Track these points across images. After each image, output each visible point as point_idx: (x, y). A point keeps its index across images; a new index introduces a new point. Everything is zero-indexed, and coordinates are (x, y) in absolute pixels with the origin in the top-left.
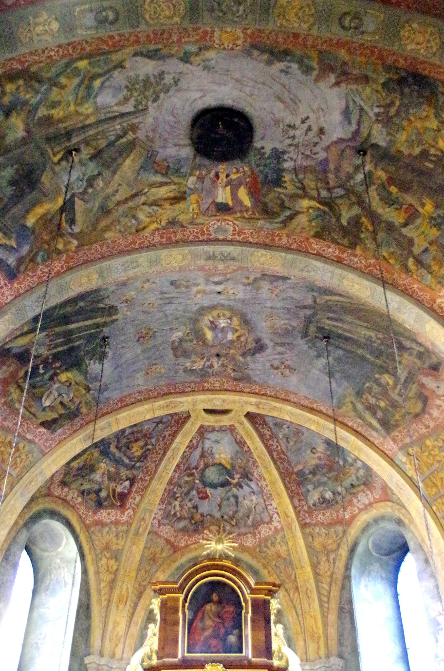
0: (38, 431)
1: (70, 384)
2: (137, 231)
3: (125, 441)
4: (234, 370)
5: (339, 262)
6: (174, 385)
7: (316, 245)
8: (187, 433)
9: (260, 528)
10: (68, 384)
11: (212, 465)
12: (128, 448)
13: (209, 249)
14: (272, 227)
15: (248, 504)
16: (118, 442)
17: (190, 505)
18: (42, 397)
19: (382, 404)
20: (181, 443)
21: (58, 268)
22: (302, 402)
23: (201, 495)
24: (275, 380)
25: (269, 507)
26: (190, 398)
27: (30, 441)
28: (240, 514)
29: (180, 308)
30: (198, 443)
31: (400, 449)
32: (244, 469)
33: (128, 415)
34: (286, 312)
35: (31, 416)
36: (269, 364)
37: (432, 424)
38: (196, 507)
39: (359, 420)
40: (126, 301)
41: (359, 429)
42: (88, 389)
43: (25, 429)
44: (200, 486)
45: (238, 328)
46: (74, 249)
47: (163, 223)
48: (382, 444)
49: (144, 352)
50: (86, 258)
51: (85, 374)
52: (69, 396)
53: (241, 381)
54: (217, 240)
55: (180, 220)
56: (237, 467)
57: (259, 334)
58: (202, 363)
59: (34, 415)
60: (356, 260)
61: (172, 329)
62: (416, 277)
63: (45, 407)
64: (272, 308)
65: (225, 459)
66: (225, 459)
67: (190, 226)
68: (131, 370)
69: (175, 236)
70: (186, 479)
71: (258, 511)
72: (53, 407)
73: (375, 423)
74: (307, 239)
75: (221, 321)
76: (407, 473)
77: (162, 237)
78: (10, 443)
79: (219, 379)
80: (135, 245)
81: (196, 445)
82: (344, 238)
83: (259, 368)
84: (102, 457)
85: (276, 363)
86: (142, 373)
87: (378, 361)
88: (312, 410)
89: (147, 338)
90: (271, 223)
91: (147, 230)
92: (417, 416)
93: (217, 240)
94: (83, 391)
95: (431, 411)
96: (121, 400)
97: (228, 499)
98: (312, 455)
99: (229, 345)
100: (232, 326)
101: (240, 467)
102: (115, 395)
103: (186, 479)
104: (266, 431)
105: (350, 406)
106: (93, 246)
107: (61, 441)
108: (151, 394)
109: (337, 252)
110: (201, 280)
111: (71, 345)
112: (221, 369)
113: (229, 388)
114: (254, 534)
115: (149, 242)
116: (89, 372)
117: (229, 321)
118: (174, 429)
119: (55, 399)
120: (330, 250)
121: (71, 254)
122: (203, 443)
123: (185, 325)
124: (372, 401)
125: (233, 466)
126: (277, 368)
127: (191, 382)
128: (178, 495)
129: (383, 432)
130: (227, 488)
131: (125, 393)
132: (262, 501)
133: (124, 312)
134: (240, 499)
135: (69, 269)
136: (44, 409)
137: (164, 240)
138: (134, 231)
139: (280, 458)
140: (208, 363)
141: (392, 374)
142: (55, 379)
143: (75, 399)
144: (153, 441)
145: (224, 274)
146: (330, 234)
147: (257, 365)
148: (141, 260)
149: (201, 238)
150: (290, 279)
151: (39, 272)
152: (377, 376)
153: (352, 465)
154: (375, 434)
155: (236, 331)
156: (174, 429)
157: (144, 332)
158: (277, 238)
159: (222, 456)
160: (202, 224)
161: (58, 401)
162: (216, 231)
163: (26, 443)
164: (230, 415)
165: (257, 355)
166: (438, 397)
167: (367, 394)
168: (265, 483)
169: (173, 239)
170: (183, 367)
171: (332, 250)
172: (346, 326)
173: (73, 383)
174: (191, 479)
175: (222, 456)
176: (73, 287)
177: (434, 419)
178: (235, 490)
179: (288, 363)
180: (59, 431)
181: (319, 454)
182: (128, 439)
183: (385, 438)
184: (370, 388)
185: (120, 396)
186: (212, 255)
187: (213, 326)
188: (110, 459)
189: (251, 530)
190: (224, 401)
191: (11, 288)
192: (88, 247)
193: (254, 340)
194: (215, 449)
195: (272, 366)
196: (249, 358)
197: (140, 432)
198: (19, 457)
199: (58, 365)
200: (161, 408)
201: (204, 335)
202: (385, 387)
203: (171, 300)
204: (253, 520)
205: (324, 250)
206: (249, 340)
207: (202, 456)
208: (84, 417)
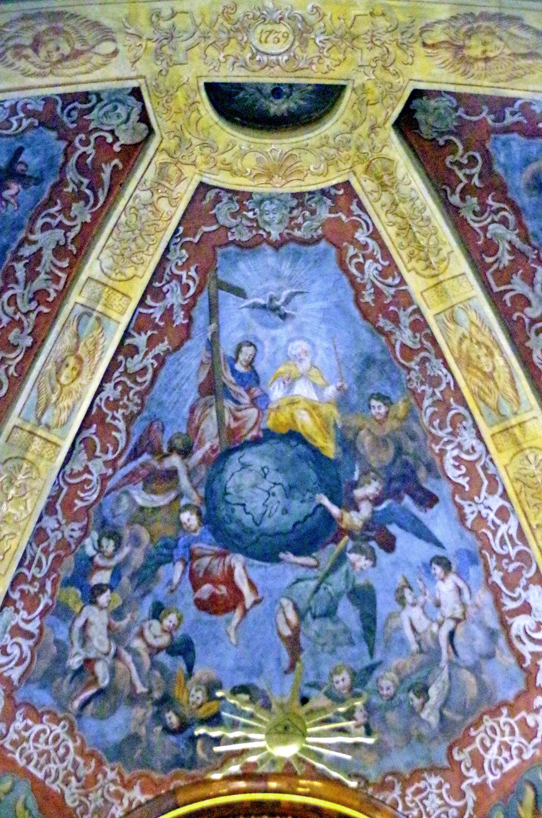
8: (140, 232)
9: (478, 734)
11: (257, 441)
15: (422, 624)
17: (156, 633)
20: (113, 282)
23: (206, 589)
25: (519, 624)
28: (387, 681)
30: (188, 309)
32: (399, 451)
38: (183, 649)
44: (206, 546)
56: (365, 441)
65: (313, 409)
66: (313, 409)
70: (142, 498)
71: (466, 656)
81: (180, 319)
97: (329, 613)
101: (380, 442)
103: (142, 498)
114: (452, 771)
118: (81, 213)
122: (213, 311)
125: (348, 444)
128: (102, 577)
130: (326, 555)
132: (484, 597)
134: (385, 605)
156: (81, 213)
159: (303, 390)
164: (331, 127)
168: (496, 502)
174: (161, 500)
175: (303, 390)
178: (359, 561)
189: (439, 752)
194: (267, 349)
204: (446, 703)
207: (210, 388)
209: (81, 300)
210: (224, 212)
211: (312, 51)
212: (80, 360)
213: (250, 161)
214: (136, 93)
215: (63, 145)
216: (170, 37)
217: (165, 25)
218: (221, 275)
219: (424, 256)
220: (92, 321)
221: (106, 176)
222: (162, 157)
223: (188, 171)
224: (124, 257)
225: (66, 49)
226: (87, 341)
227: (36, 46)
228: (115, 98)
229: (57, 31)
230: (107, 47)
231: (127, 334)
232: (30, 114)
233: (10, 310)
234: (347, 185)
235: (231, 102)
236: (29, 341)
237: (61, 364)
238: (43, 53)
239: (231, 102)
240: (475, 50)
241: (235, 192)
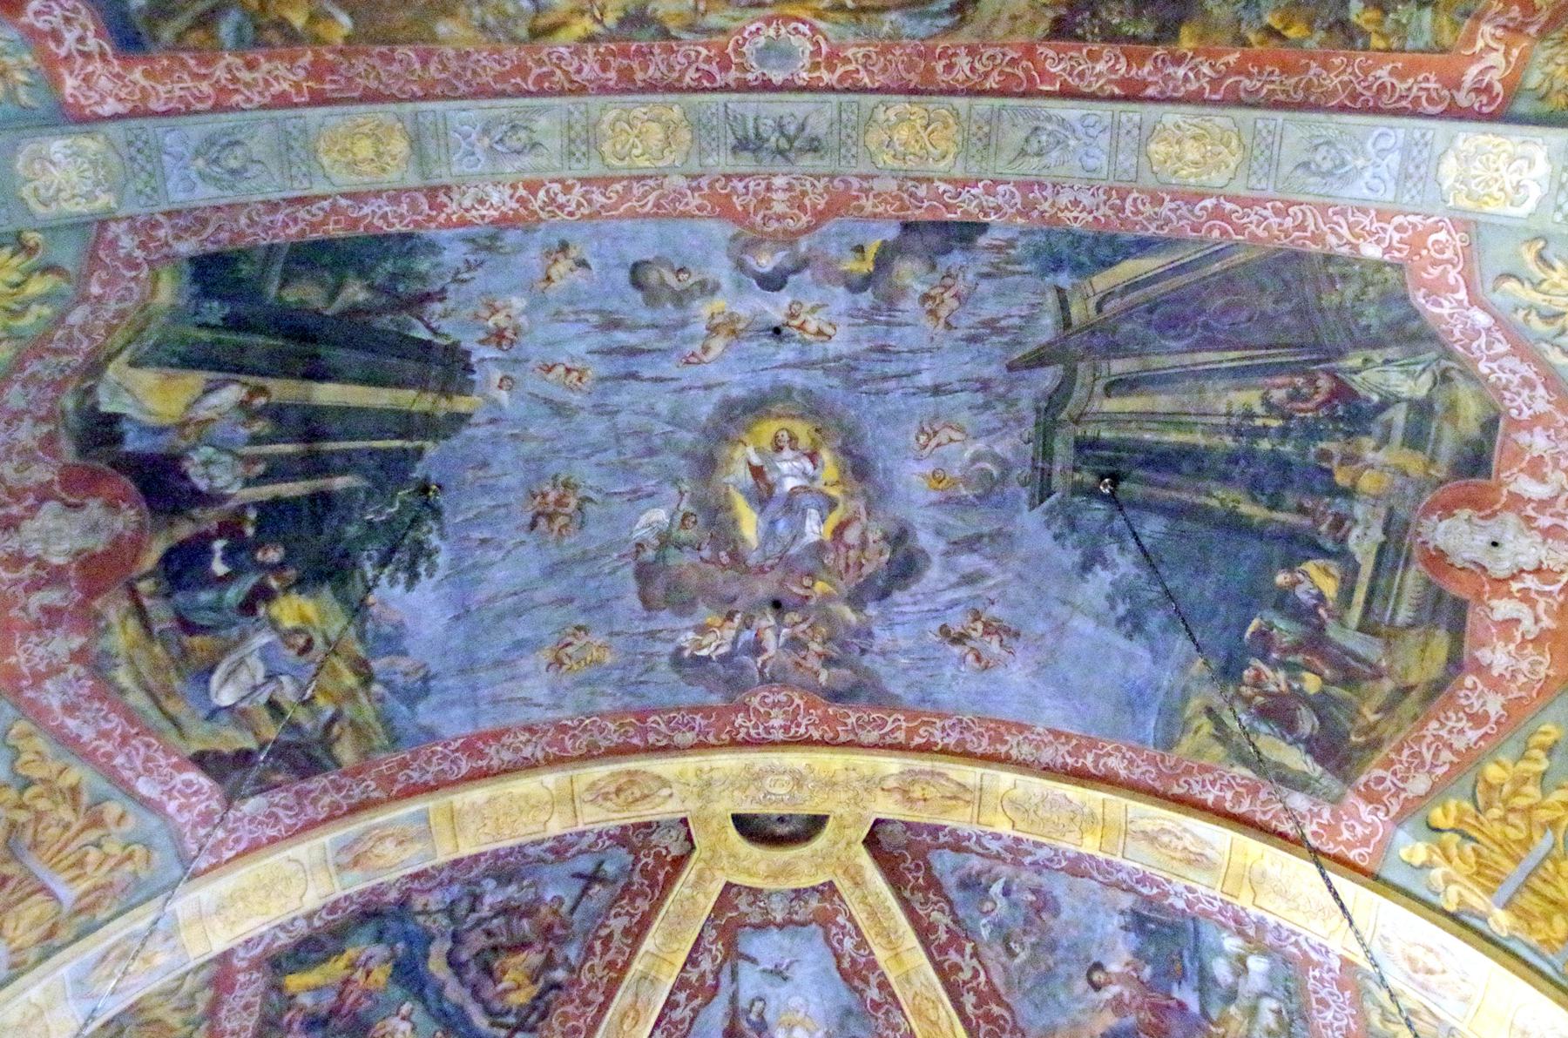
1: (310, 642)
2: (536, 34)
3: (477, 941)
4: (828, 661)
5: (1132, 93)
6: (642, 715)
7: (1057, 64)
8: (684, 917)
10: (301, 641)
12: (488, 970)
13: (740, 109)
14: (923, 28)
16: (456, 938)
18: (211, 671)
19: (1311, 684)
20: (662, 955)
21: (286, 86)
22: (1047, 756)
24: (956, 682)
26: (688, 764)
27: (145, 803)
29: (663, 407)
30: (717, 974)
31: (1398, 821)
33: (491, 801)
34: (980, 398)
35: (165, 724)
36: (935, 626)
37: (1494, 705)
39: (1241, 771)
40: (498, 336)
41: (1244, 808)
42: (367, 679)
43: (138, 763)
45: (834, 492)
46: (339, 42)
47: (611, 20)
48: (1332, 830)
49: (551, 572)
50: (373, 84)
51: (358, 611)
53: (850, 702)
54: (767, 86)
55: (660, 13)
57: (899, 510)
58: (729, 634)
59: (175, 722)
60: (1181, 72)
61: (636, 495)
62: (1381, 44)
63: (220, 709)
64: (936, 390)
67: (686, 36)
68: (507, 639)
69: (645, 69)
72: (244, 713)
73: (1296, 759)
74: (1029, 52)
75: (785, 467)
76: (1440, 902)
77: (605, 67)
78: (74, 791)
79: (782, 697)
80: (525, 80)
81: (710, 981)
82: (1137, 15)
83: (903, 644)
84: (397, 992)
85: (957, 621)
86: (545, 656)
87: (1280, 516)
88: (1080, 776)
89: (561, 520)
90: (923, 15)
91: (562, 36)
92: (1436, 690)
93: (767, 86)
94: (350, 680)
95: (1484, 655)
96: (470, 747)
98: (1093, 995)
99: (809, 564)
100: (818, 485)
102: (454, 724)
104: (936, 915)
105: (1207, 727)
106: (401, 51)
107: (254, 847)
108: (568, 743)
109: (1122, 66)
110: (721, 270)
111: (319, 483)
112: (787, 659)
113: (816, 735)
115: (566, 73)
116: (374, 610)
117: (809, 467)
118: (643, 905)
120: (1101, 67)
121: (330, 57)
123: (676, 482)
124: (1276, 680)
126: (960, 639)
127: (695, 710)
129: (1328, 781)
131: (486, 725)
133: (491, 391)
135: (318, 100)
136: (214, 713)
137: (612, 75)
138: (522, 32)
139: (989, 1018)
140: (748, 635)
141: (1328, 554)
142: (262, 611)
143: (321, 701)
144: (573, 952)
145: (791, 238)
146: (1094, 15)
147: (901, 632)
148: (542, 123)
149: (720, 80)
150: (983, 228)
151: (220, 73)
152: (1281, 578)
153: (1231, 996)
154: (1299, 801)
155: (832, 504)
156: (643, 905)
157: (552, 497)
158: (940, 66)
160: (723, 31)
161: (263, 699)
162: (764, 54)
163: (130, 806)
164: (820, 842)
165: (898, 596)
166: (1500, 585)
167: (1258, 663)
169: (639, 76)
170: (670, 648)
171: (1106, 66)
172: (1163, 402)
173: (318, 641)
176: (326, 161)
177: (1496, 685)
179: (994, 611)
180: (253, 805)
181: (1114, 990)
182: (489, 934)
183: (1336, 801)
184: (1264, 635)
185: (469, 730)
186: (752, 136)
187: (762, 491)
188: (428, 1009)
190: (798, 780)
191: (118, 76)
192: (384, 49)
193: (885, 538)
194: (773, 1004)
195: (944, 631)
196: (872, 610)
197: (529, 911)
198: (98, 845)
199: (274, 555)
200: (600, 795)
201: (735, 522)
202: (1313, 611)
203: (635, 364)
205: (1081, 75)
206: (871, 537)
208: (346, 781)
209: (640, 967)
210: (743, 903)
211: (805, 793)
212: (637, 1012)
213: (762, 867)
214: (684, 821)
215: (631, 858)
216: (709, 784)
217: (705, 777)
218: (742, 949)
219: (887, 934)
220: (647, 983)
221: (661, 877)
222: (701, 865)
223: (718, 874)
224: (671, 936)
225: (638, 794)
226: (643, 997)
227: (618, 791)
228: (670, 826)
229: (632, 782)
230: (666, 792)
231: (671, 993)
232: (610, 837)
233: (589, 976)
234: (831, 884)
235: (748, 827)
236: (602, 999)
237: (624, 1015)
238: (622, 796)
239: (748, 827)
240: (917, 792)
241: (751, 889)
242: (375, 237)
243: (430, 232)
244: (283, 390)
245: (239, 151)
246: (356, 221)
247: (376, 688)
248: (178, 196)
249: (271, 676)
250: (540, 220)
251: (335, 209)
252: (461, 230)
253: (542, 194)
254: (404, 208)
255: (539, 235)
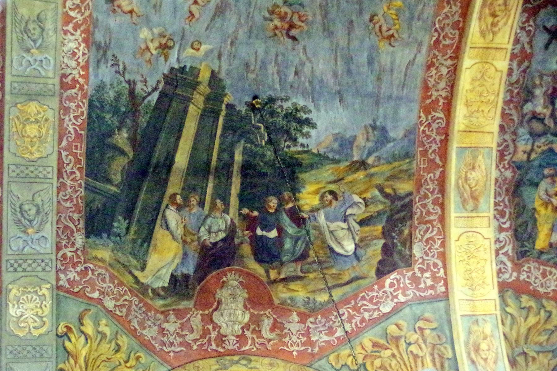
0: (387, 288)
1: (331, 192)
10: (329, 197)
18: (332, 250)
27: (395, 311)
33: (468, 104)
35: (354, 285)
40: (164, 48)
42: (363, 165)
43: (371, 306)
49: (328, 32)
52: (356, 204)
59: (357, 278)
63: (355, 253)
72: (362, 240)
78: (375, 345)
86: (384, 46)
89: (296, 20)
94: (360, 175)
96: (427, 110)
102: (409, 115)
107: (443, 256)
108: (448, 42)
119: (349, 229)
131: (417, 95)
133: (200, 57)
136: (356, 256)
142: (305, 215)
143: (368, 195)
157: (277, 22)
161: (357, 227)
163: (394, 319)
173: (332, 187)
176: (37, 155)
180: (417, 251)
185: (416, 107)
198: (409, 344)
199: (273, 202)
208: (423, 191)
242: (89, 124)
243: (90, 89)
244: (174, 185)
245: (26, 207)
246: (78, 136)
247: (370, 161)
248: (48, 247)
249: (345, 220)
250: (90, 16)
251: (68, 148)
252: (91, 69)
253: (72, 14)
254: (73, 105)
255: (100, 18)
